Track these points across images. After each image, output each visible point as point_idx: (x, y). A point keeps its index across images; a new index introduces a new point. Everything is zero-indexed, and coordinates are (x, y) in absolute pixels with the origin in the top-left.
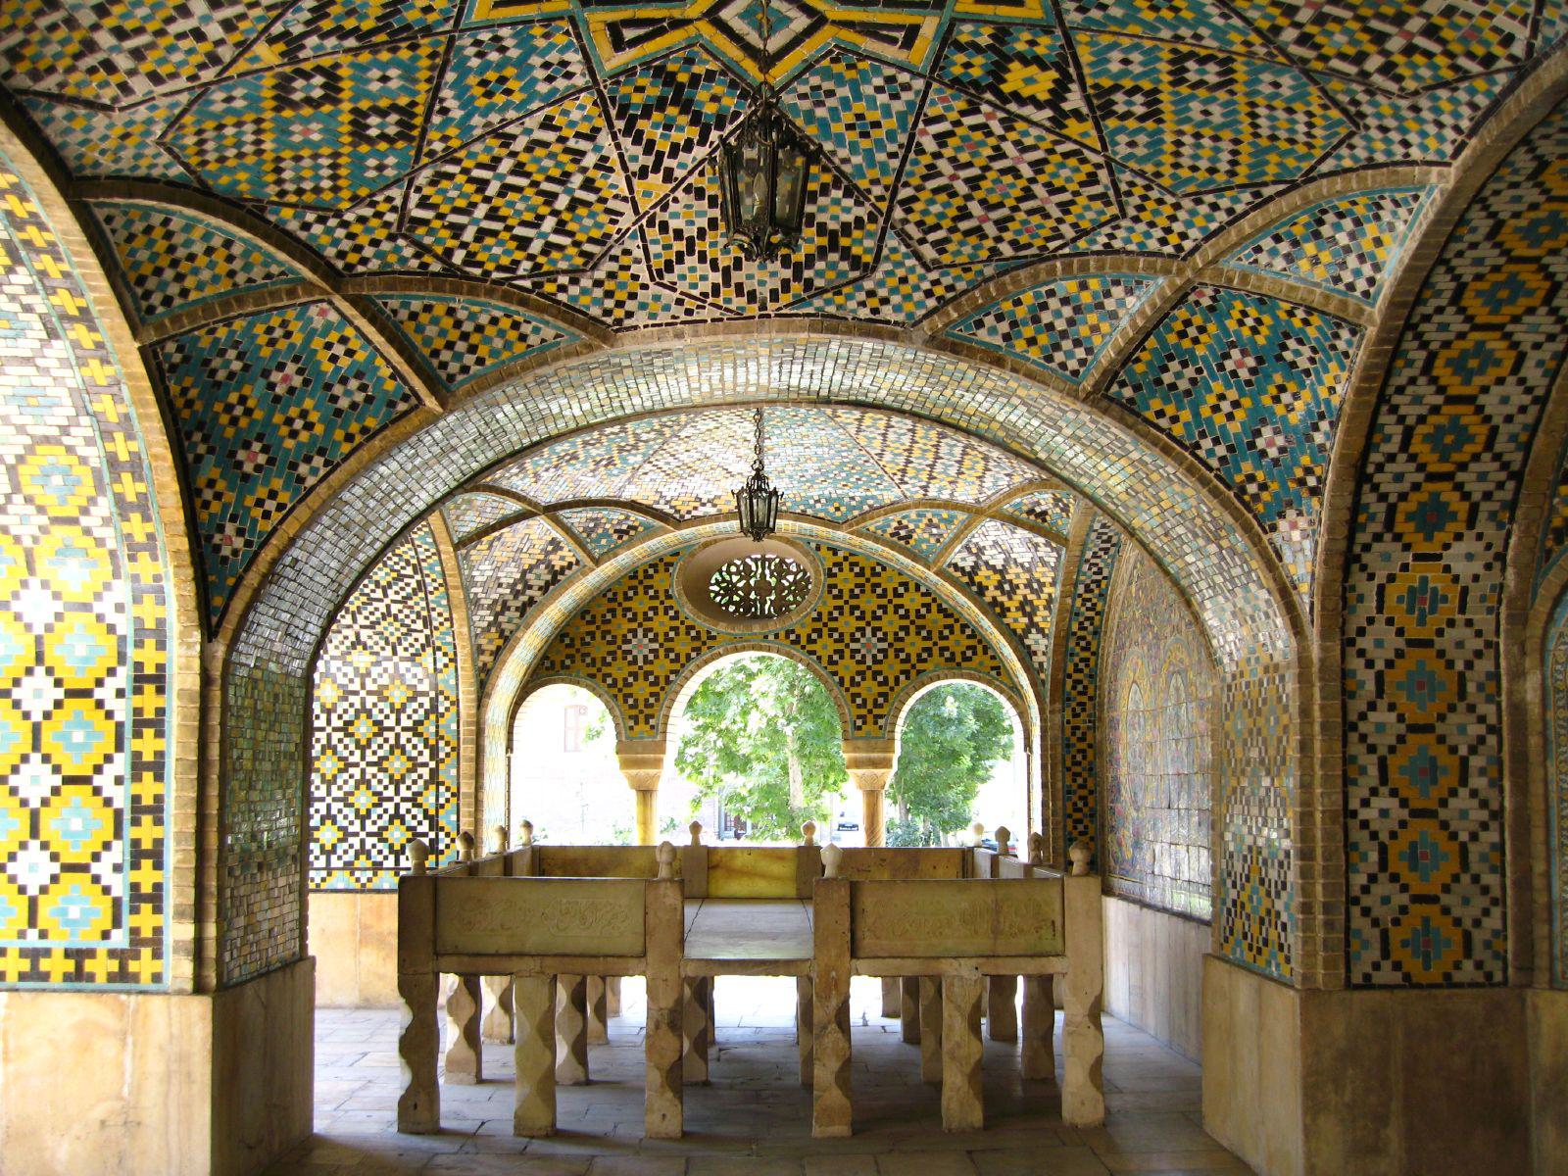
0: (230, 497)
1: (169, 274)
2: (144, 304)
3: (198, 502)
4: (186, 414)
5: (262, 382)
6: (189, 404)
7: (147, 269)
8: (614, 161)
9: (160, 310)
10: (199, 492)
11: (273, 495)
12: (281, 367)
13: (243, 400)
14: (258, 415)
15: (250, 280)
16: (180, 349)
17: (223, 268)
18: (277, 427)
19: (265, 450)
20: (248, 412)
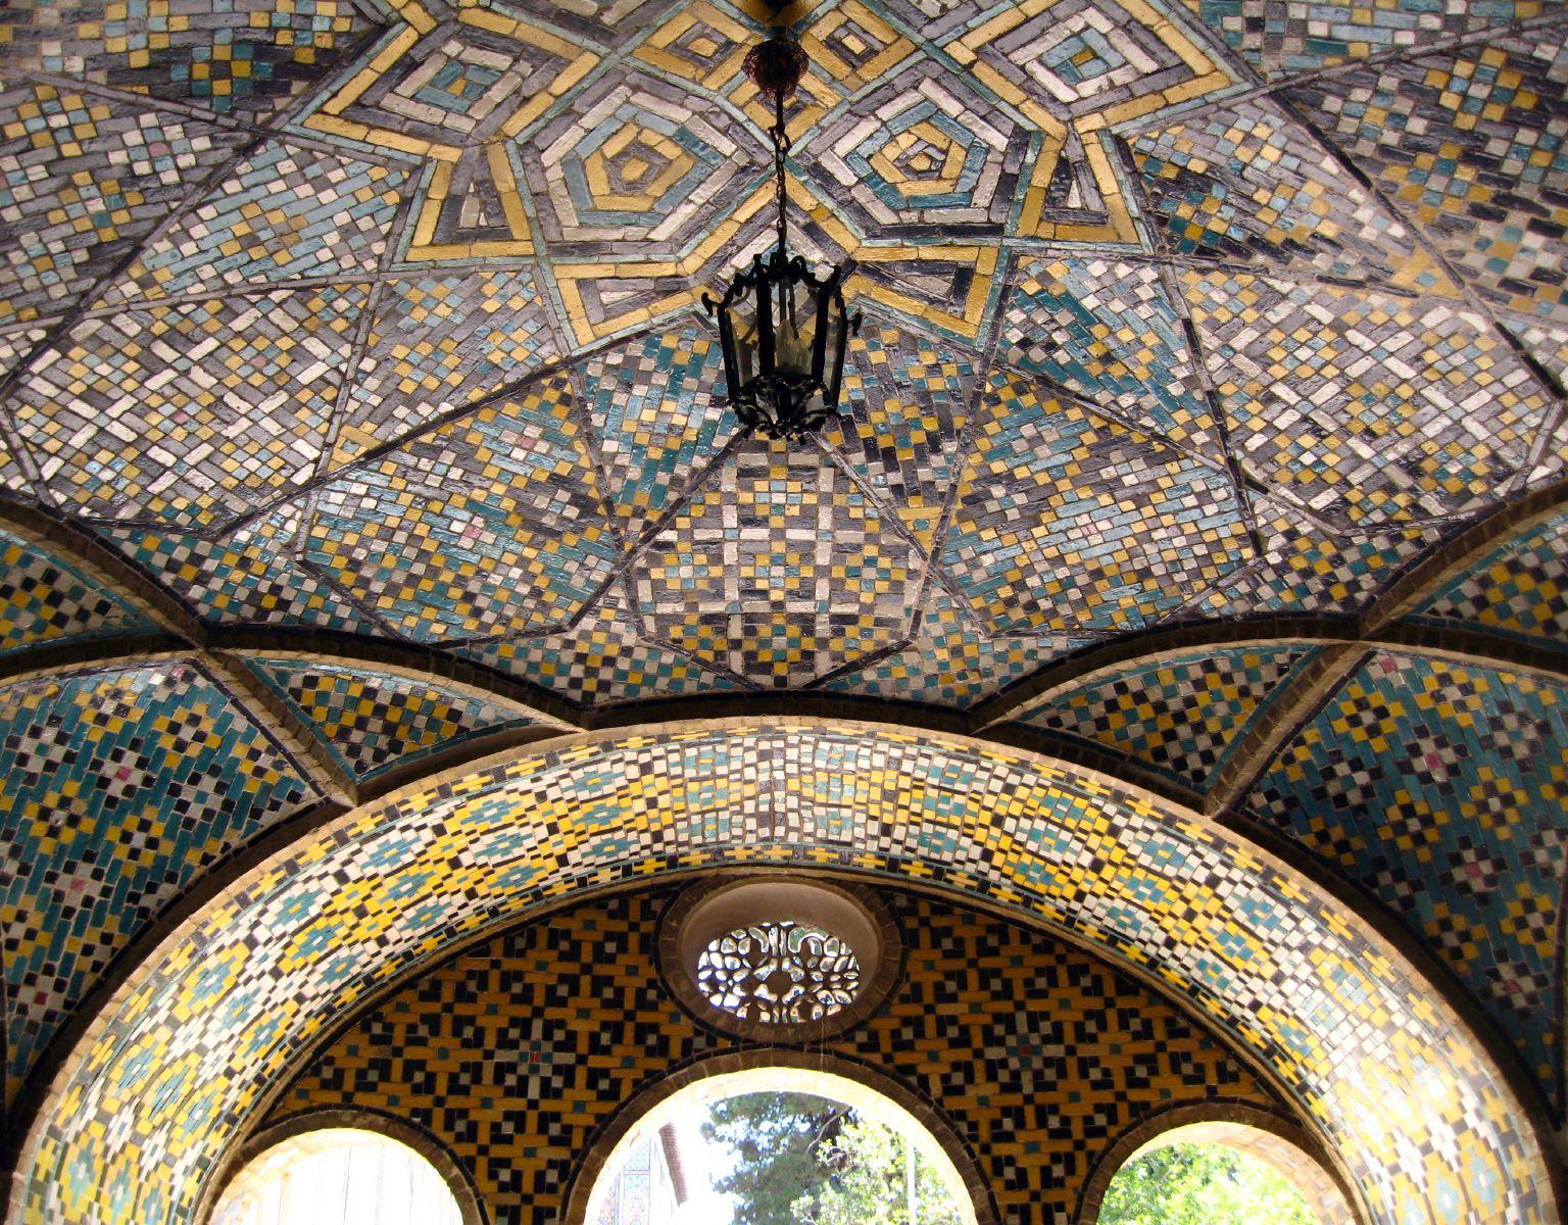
0: (1479, 931)
1: (1184, 731)
2: (1187, 774)
3: (1444, 955)
4: (1347, 859)
5: (1410, 780)
6: (1343, 846)
7: (1155, 740)
8: (1337, 293)
9: (1208, 770)
10: (1437, 942)
11: (1530, 906)
12: (1415, 751)
13: (1408, 810)
14: (1441, 818)
15: (1268, 686)
16: (1272, 796)
17: (1230, 692)
18: (1474, 821)
19: (1482, 855)
20: (1427, 821)
